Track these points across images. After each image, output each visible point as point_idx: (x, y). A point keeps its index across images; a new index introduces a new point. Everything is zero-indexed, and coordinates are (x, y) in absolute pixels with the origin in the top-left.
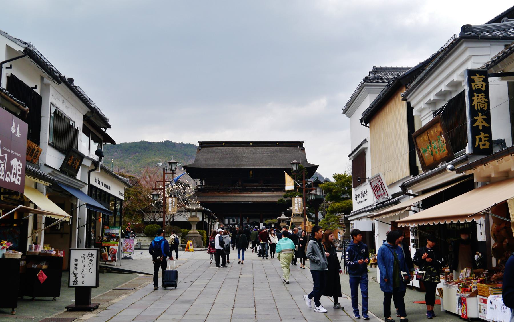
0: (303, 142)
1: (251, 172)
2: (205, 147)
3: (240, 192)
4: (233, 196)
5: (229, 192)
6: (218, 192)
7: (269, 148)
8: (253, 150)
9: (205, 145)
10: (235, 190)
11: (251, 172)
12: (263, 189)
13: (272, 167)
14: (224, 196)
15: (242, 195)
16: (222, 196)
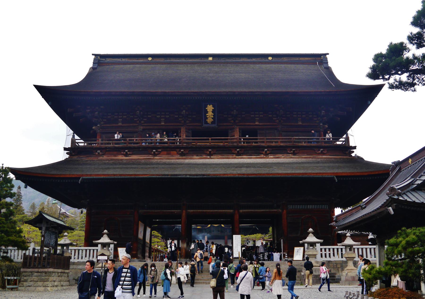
0: (325, 55)
1: (210, 108)
2: (108, 64)
3: (182, 154)
4: (165, 164)
5: (155, 155)
6: (126, 155)
7: (252, 66)
8: (216, 68)
9: (108, 60)
10: (168, 149)
11: (210, 108)
12: (242, 147)
13: (264, 90)
14: (139, 164)
15: (187, 161)
16: (134, 164)
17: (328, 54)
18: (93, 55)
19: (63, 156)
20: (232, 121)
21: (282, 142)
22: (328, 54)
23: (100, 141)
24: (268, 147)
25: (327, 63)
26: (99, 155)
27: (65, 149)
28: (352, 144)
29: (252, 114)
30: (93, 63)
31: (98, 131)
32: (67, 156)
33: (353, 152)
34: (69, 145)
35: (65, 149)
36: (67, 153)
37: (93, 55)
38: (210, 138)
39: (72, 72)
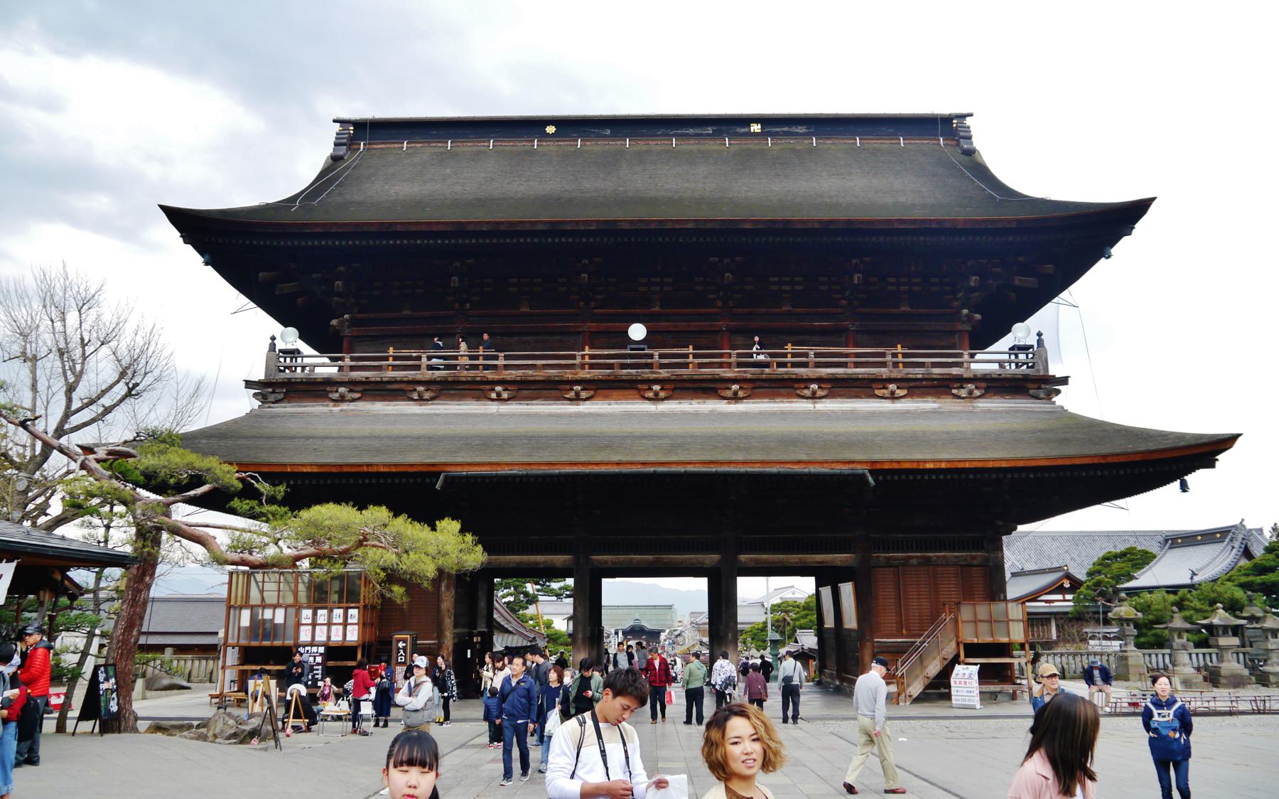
0: (964, 116)
17: (971, 115)
18: (335, 121)
19: (244, 404)
20: (719, 303)
21: (857, 365)
22: (971, 115)
23: (348, 362)
24: (819, 380)
25: (970, 138)
26: (343, 399)
27: (249, 384)
28: (1055, 370)
29: (775, 283)
30: (336, 145)
31: (347, 332)
32: (256, 404)
33: (1058, 392)
34: (259, 374)
35: (249, 384)
36: (255, 395)
37: (335, 121)
38: (656, 354)
39: (275, 166)
